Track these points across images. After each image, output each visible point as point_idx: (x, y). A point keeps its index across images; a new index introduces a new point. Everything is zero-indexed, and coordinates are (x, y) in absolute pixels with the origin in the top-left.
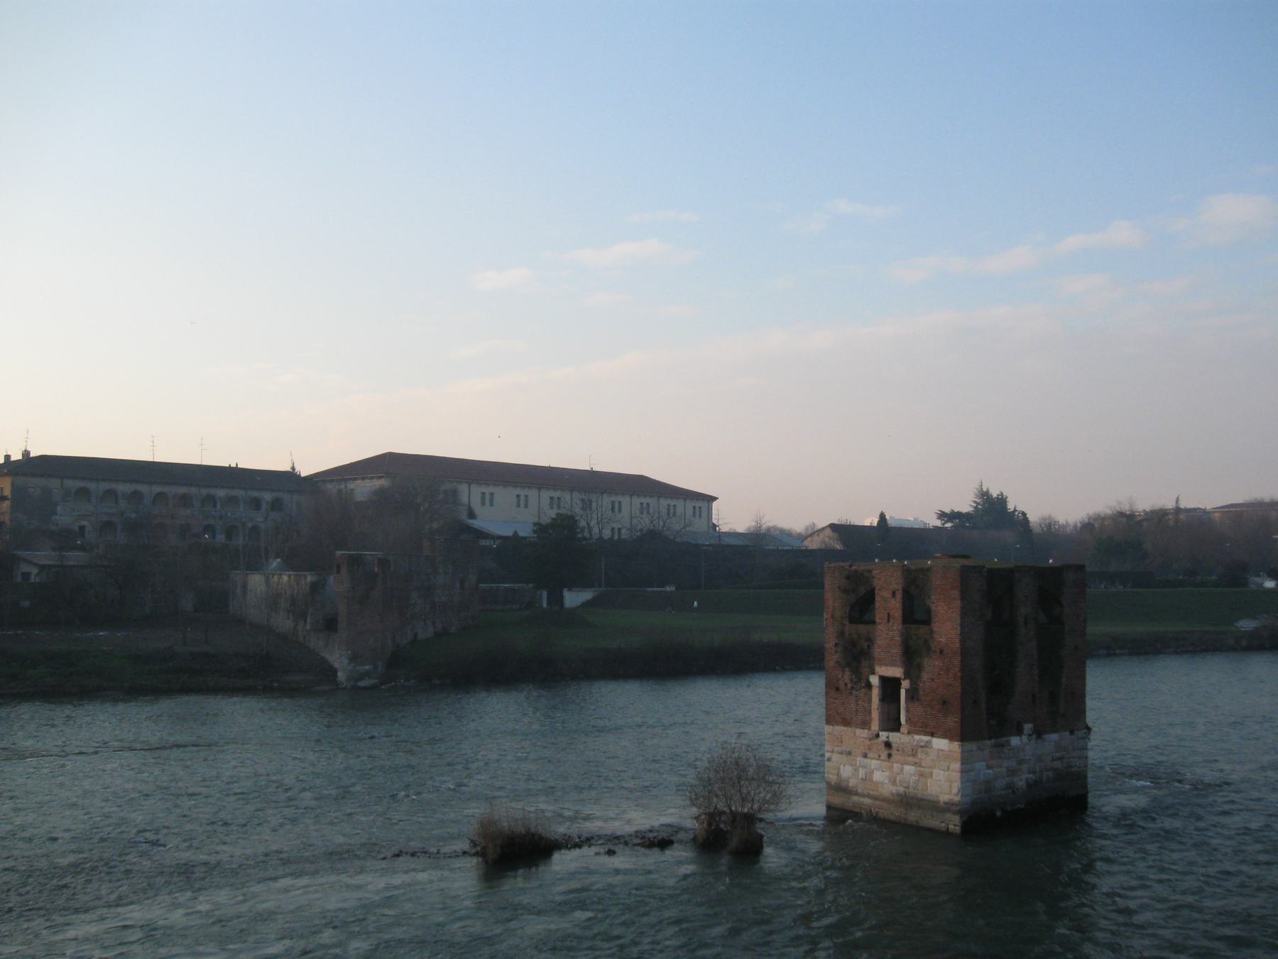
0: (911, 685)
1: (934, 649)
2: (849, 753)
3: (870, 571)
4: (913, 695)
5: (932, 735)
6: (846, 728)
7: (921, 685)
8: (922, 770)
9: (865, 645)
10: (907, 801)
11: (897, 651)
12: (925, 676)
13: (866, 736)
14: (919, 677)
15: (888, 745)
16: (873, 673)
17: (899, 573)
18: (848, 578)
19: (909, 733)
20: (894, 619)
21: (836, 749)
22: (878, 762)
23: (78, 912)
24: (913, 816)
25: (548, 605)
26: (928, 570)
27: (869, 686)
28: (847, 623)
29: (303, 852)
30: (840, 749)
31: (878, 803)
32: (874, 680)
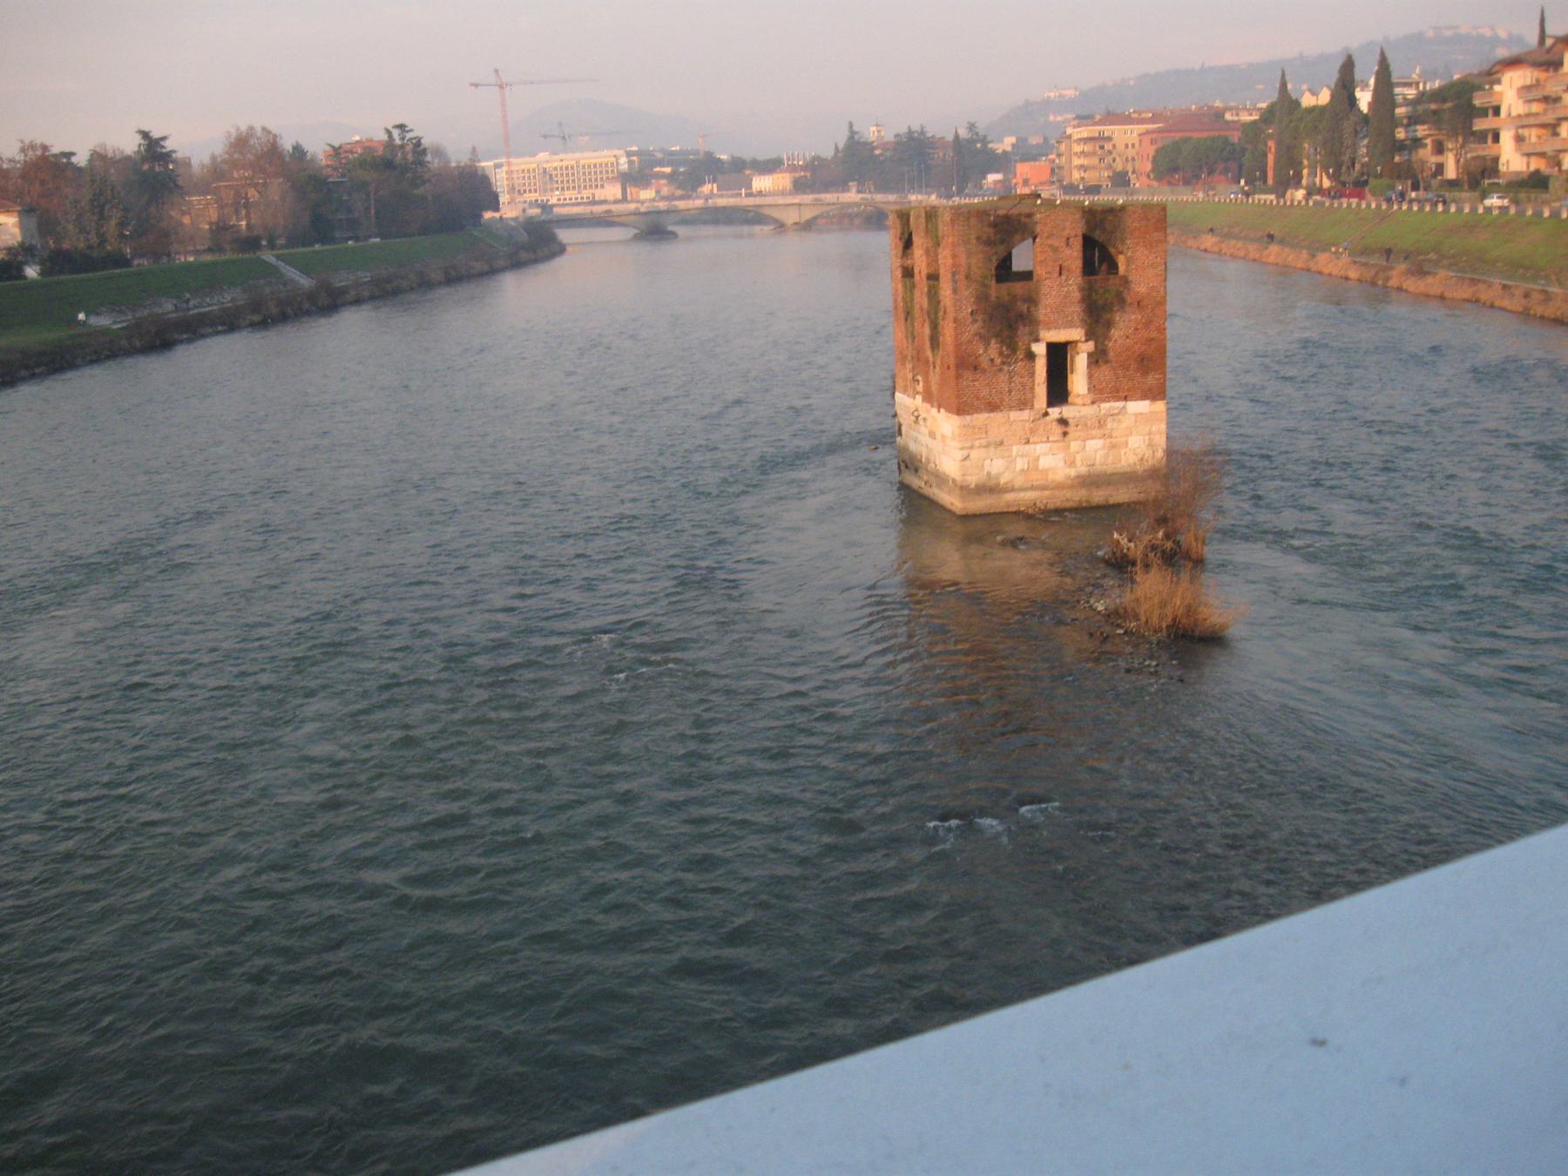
0: (1096, 347)
1: (1129, 301)
2: (1001, 443)
3: (1030, 215)
4: (1096, 359)
5: (1126, 399)
6: (992, 415)
7: (1110, 345)
8: (1114, 440)
9: (1024, 308)
10: (1091, 480)
11: (1076, 310)
12: (1115, 333)
13: (1027, 418)
14: (1107, 337)
15: (1063, 422)
16: (1037, 340)
17: (1078, 216)
18: (995, 225)
19: (1093, 403)
20: (1068, 270)
21: (977, 443)
22: (1049, 445)
23: (1293, 709)
24: (1098, 496)
25: (308, 275)
26: (1120, 210)
27: (1031, 356)
28: (993, 282)
29: (227, 783)
30: (984, 442)
31: (1047, 493)
32: (1040, 349)
